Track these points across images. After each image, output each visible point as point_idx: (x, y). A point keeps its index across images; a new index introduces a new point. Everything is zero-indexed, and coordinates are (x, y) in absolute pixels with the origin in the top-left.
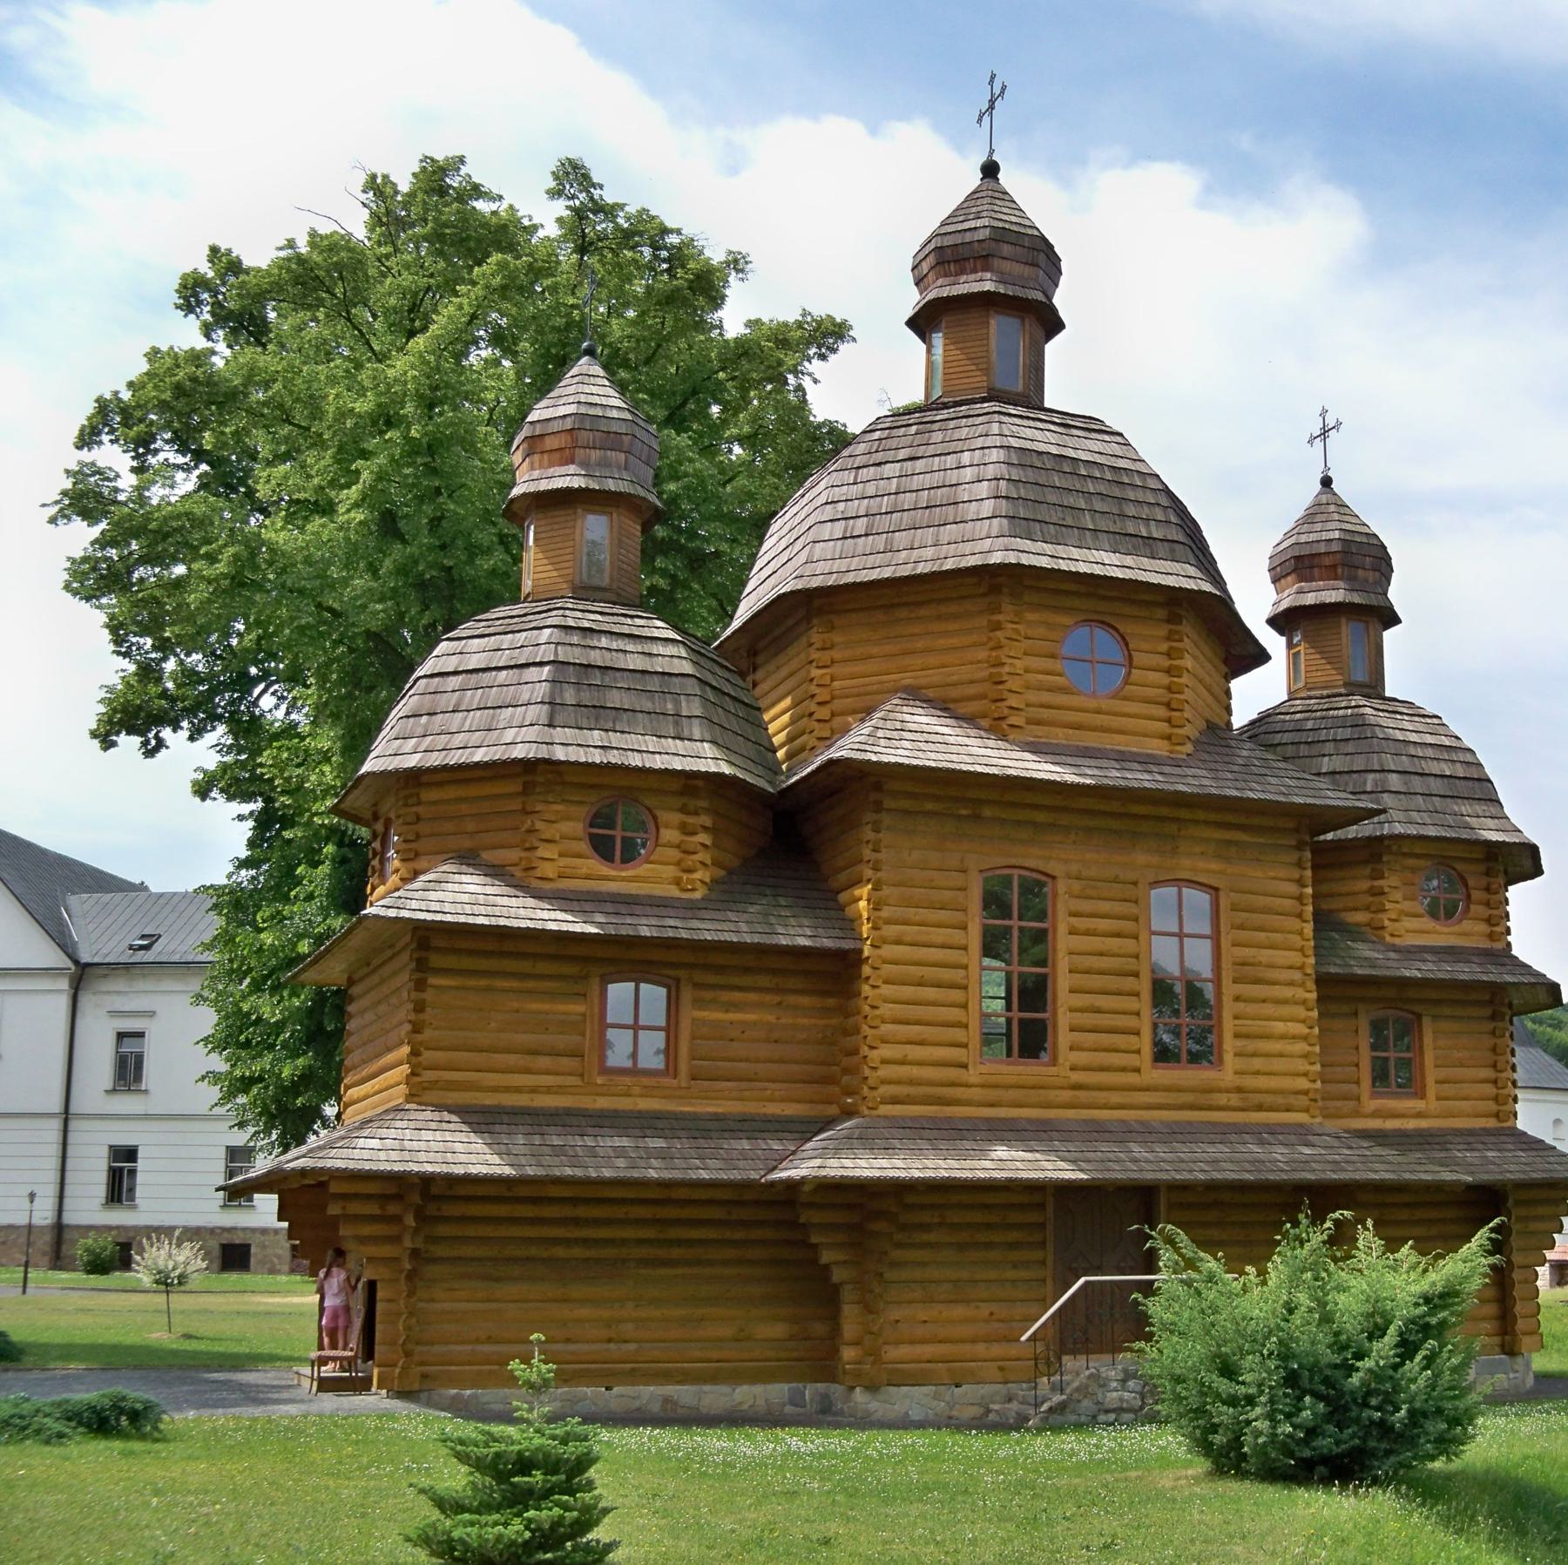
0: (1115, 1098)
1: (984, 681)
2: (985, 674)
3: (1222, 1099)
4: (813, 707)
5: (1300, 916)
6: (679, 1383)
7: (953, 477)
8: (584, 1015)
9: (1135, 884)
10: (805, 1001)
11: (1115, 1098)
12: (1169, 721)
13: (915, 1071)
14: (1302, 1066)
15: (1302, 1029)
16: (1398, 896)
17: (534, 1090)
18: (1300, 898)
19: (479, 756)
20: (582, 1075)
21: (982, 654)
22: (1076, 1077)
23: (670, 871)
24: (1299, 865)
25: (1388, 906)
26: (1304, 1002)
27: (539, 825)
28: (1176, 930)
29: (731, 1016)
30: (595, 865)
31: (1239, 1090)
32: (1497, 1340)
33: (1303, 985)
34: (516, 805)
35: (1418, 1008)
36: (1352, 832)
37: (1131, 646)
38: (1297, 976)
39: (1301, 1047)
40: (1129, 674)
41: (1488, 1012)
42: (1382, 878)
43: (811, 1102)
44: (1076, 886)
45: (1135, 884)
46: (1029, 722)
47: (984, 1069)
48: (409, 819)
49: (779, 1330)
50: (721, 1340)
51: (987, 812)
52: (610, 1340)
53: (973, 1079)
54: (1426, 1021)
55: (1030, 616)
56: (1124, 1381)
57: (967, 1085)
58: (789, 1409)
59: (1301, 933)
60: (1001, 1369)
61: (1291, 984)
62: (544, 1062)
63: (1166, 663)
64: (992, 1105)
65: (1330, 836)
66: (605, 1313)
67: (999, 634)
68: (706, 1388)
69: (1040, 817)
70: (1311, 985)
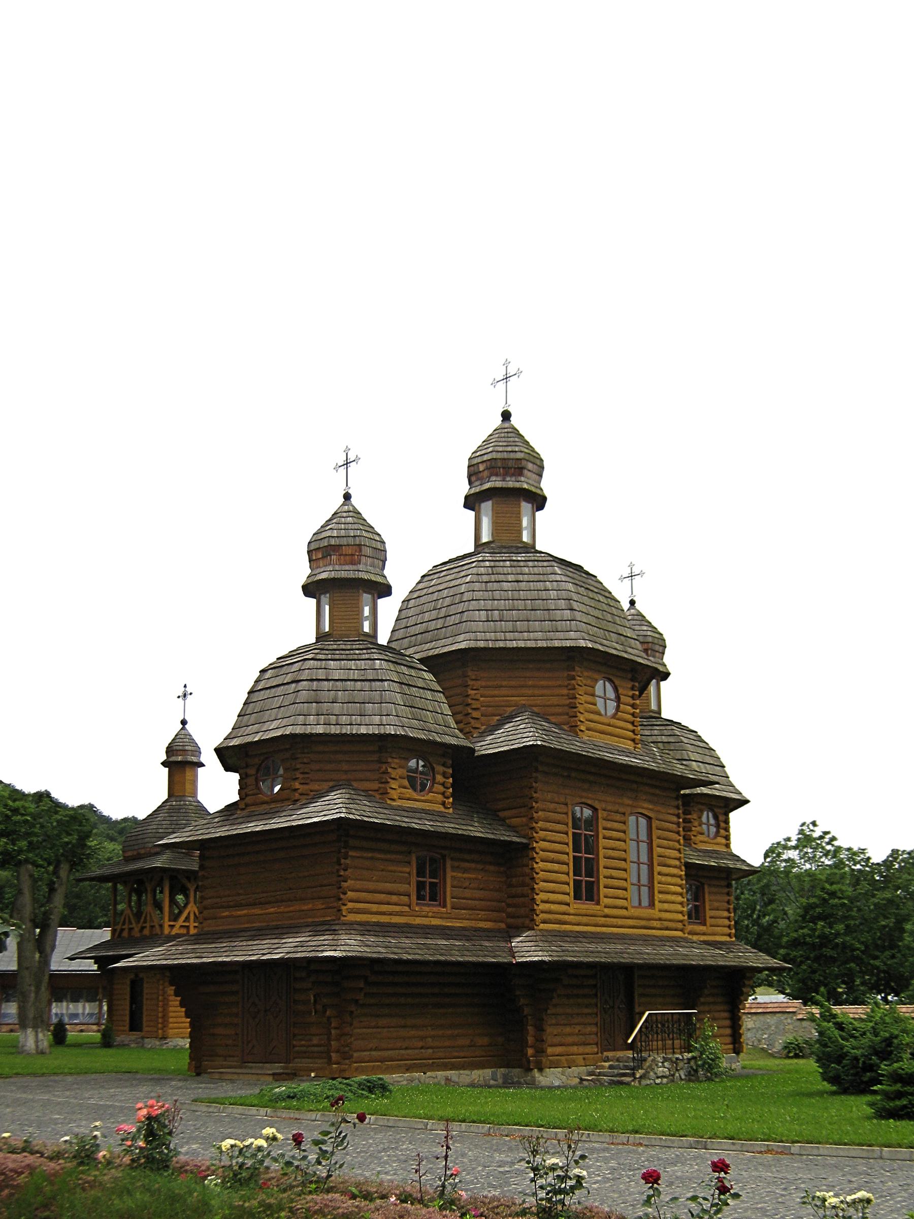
0: (620, 922)
1: (564, 706)
2: (568, 702)
3: (655, 924)
4: (470, 711)
5: (678, 833)
6: (451, 1069)
7: (544, 594)
8: (409, 873)
9: (624, 814)
10: (492, 868)
11: (620, 922)
12: (633, 731)
13: (553, 907)
14: (679, 908)
15: (678, 889)
16: (696, 824)
17: (391, 914)
18: (678, 824)
19: (363, 730)
20: (409, 906)
21: (565, 691)
22: (607, 911)
23: (440, 798)
24: (678, 807)
25: (693, 829)
26: (680, 876)
27: (389, 770)
28: (635, 838)
29: (466, 875)
30: (410, 792)
31: (660, 919)
32: (731, 1046)
33: (680, 868)
34: (375, 757)
35: (703, 880)
36: (698, 790)
37: (621, 691)
38: (677, 863)
39: (680, 899)
40: (618, 707)
41: (724, 883)
42: (690, 814)
43: (495, 921)
44: (605, 814)
45: (624, 814)
46: (588, 729)
47: (576, 906)
48: (305, 760)
49: (485, 1040)
50: (463, 1046)
51: (573, 774)
52: (422, 1048)
53: (572, 911)
54: (706, 887)
55: (586, 674)
56: (662, 1063)
57: (569, 914)
58: (492, 1082)
59: (678, 842)
60: (584, 1059)
61: (675, 867)
62: (394, 898)
63: (632, 702)
64: (578, 925)
65: (687, 791)
66: (421, 1033)
67: (573, 682)
68: (462, 1072)
69: (592, 778)
70: (683, 868)
